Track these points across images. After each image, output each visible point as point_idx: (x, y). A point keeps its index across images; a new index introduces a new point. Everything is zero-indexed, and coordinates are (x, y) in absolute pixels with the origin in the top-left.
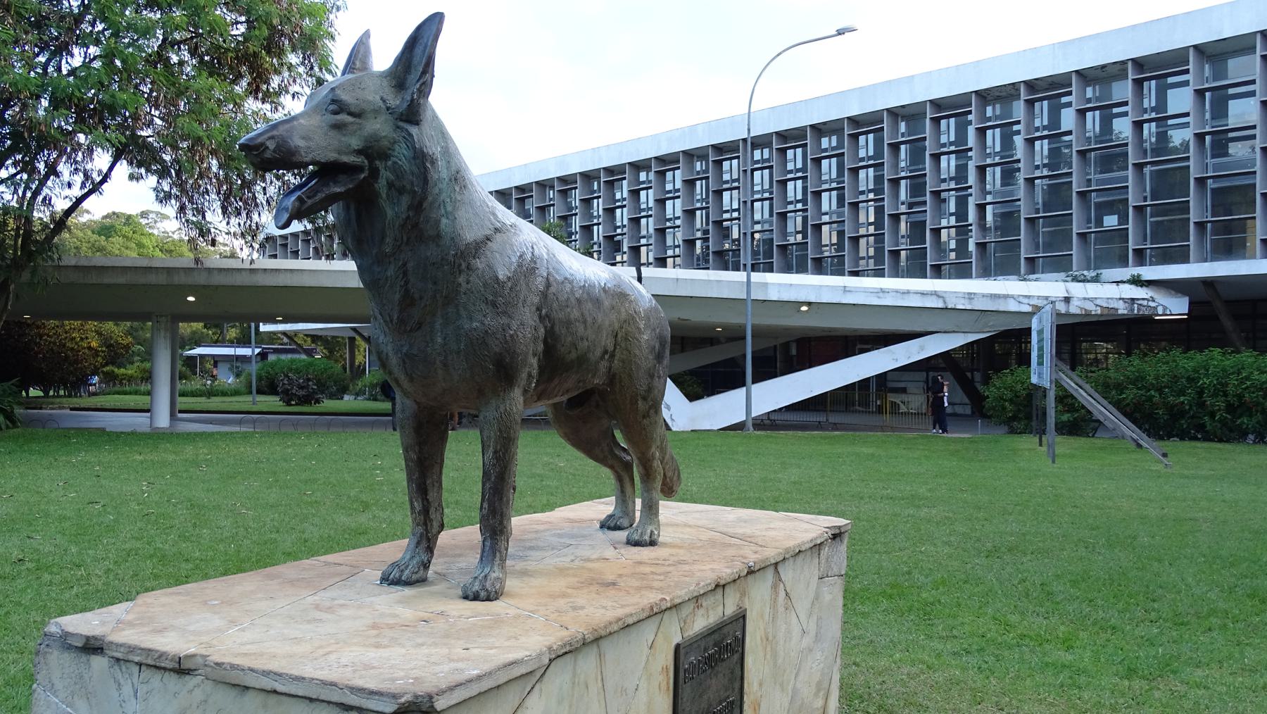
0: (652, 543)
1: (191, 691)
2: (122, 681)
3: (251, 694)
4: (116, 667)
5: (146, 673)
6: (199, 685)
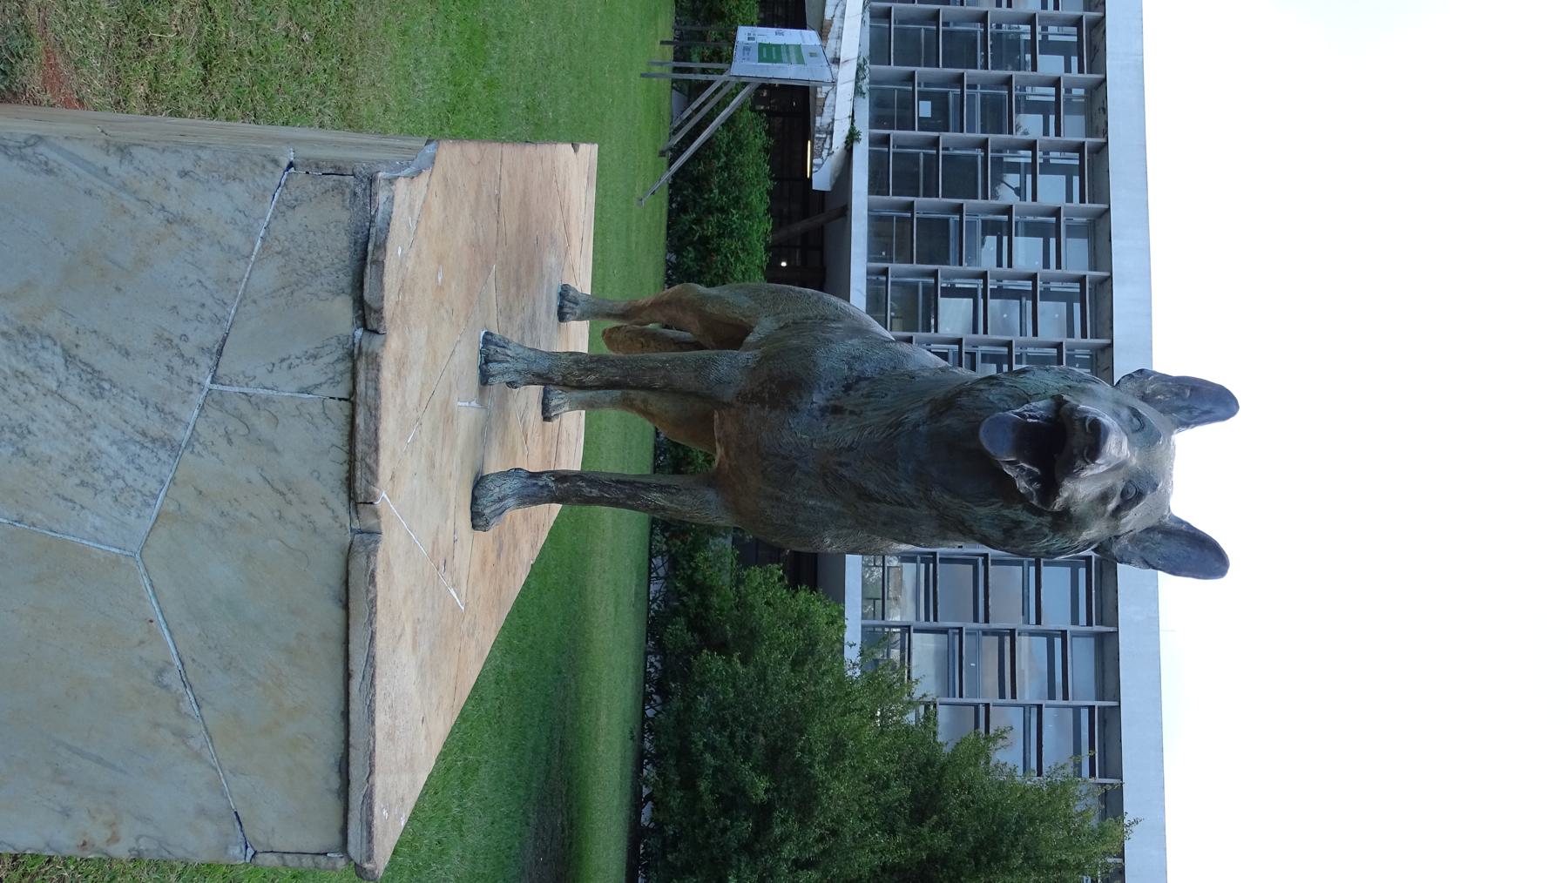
0: (547, 418)
1: (325, 504)
2: (320, 362)
3: (338, 613)
4: (340, 353)
5: (339, 412)
6: (336, 518)
